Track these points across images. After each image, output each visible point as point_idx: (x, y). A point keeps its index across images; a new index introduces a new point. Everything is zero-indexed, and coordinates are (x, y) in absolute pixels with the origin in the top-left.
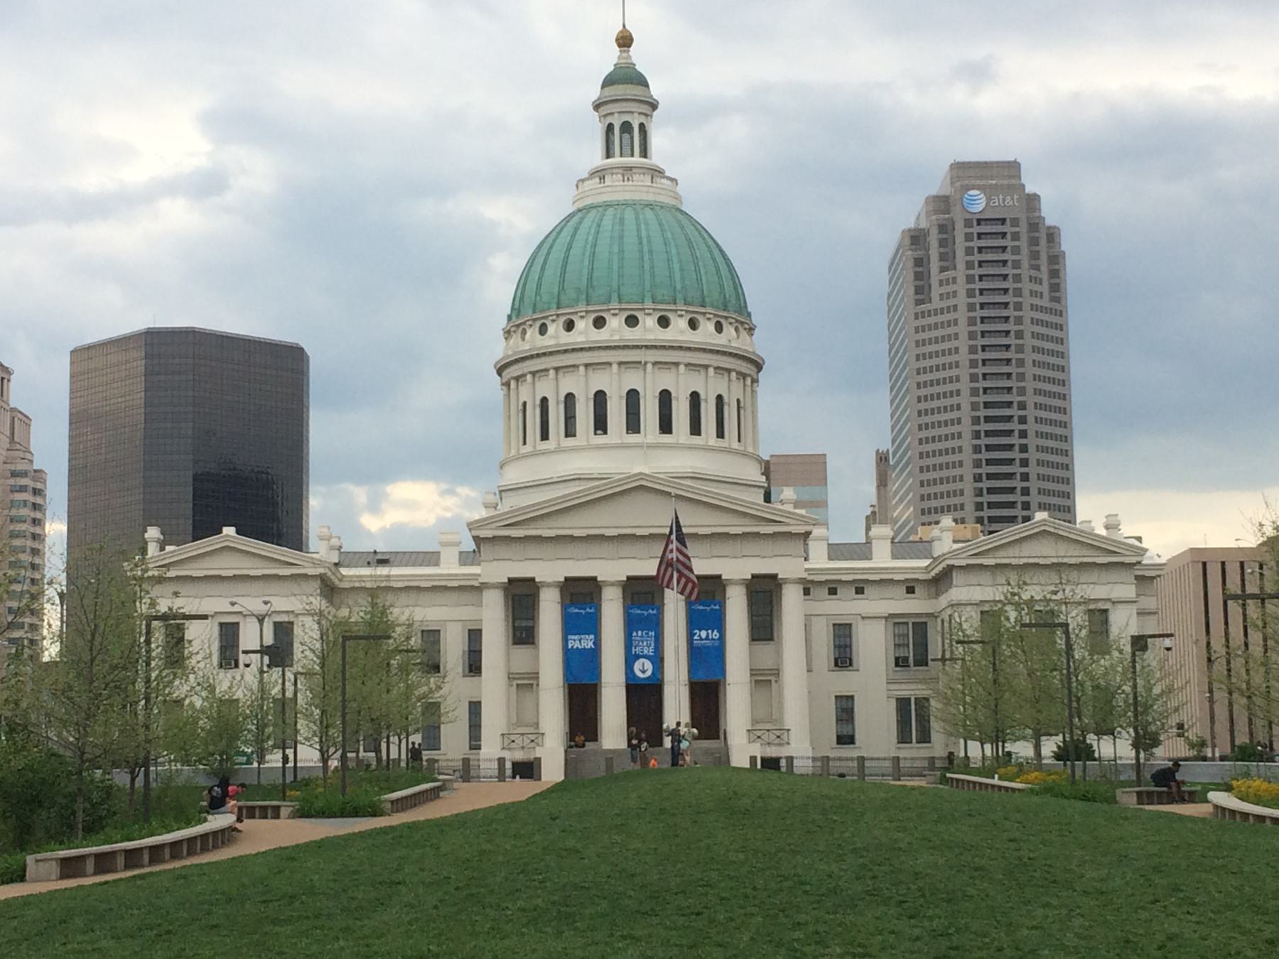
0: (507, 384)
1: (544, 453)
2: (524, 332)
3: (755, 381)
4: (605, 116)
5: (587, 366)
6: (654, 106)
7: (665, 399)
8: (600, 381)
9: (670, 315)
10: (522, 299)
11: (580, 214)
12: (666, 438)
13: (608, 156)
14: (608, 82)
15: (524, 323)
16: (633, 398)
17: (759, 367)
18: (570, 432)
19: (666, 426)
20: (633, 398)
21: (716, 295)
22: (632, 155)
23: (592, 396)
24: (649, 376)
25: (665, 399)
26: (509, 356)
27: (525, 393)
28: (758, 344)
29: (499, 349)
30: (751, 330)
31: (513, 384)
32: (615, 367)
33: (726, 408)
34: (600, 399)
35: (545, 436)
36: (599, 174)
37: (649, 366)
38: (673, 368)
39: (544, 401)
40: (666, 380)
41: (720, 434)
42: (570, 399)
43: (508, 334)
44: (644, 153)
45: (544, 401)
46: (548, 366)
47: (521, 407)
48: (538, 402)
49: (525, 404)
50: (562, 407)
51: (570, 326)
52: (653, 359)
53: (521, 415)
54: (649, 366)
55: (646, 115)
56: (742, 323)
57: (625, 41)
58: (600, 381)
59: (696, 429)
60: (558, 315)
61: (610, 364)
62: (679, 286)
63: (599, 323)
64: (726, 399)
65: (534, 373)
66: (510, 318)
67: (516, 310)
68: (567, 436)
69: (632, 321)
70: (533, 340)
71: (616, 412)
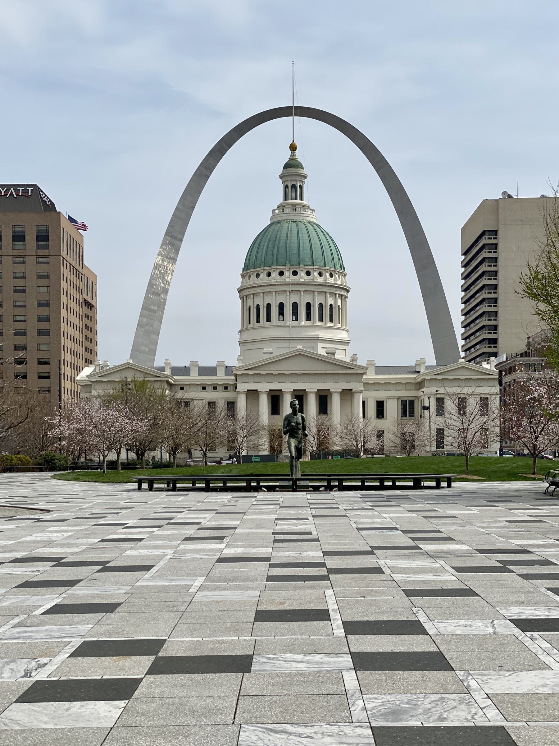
0: (242, 298)
1: (257, 328)
2: (250, 277)
3: (346, 297)
5: (276, 292)
6: (305, 177)
7: (308, 306)
8: (281, 299)
9: (311, 271)
10: (249, 262)
11: (273, 226)
12: (309, 323)
13: (285, 200)
14: (287, 166)
15: (250, 272)
16: (295, 306)
17: (348, 291)
18: (269, 319)
19: (309, 317)
20: (295, 306)
21: (330, 262)
22: (296, 199)
23: (278, 304)
24: (302, 297)
25: (308, 306)
26: (244, 286)
27: (250, 302)
28: (348, 282)
29: (238, 282)
30: (345, 275)
31: (245, 298)
33: (334, 309)
34: (281, 306)
35: (258, 321)
36: (281, 207)
37: (302, 293)
38: (312, 293)
39: (258, 306)
40: (308, 298)
41: (331, 321)
42: (269, 306)
43: (243, 276)
44: (301, 199)
45: (258, 306)
46: (259, 291)
48: (255, 306)
49: (250, 307)
50: (265, 309)
51: (269, 275)
53: (248, 311)
54: (302, 293)
56: (341, 273)
57: (293, 148)
59: (321, 319)
60: (264, 270)
61: (286, 291)
63: (281, 274)
64: (334, 306)
65: (253, 294)
66: (244, 269)
68: (267, 321)
69: (295, 273)
71: (288, 310)
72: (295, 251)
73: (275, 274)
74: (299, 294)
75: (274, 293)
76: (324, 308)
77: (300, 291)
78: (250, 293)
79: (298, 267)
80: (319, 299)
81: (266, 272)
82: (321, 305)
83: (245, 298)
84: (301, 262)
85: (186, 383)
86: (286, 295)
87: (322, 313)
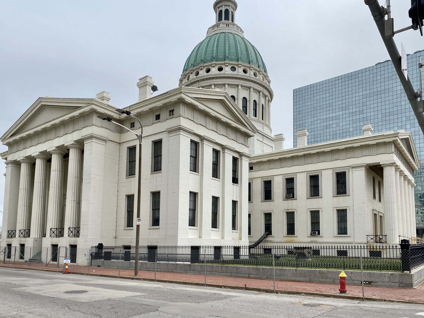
4: (219, 8)
9: (248, 69)
24: (240, 91)
32: (227, 86)
36: (217, 25)
37: (240, 87)
44: (233, 20)
51: (208, 71)
52: (241, 84)
55: (234, 9)
60: (204, 67)
61: (224, 85)
62: (250, 60)
63: (220, 69)
67: (185, 70)
69: (233, 69)
70: (193, 77)
72: (233, 50)
73: (214, 71)
75: (213, 86)
77: (237, 86)
79: (236, 63)
81: (205, 69)
84: (239, 59)
86: (225, 88)
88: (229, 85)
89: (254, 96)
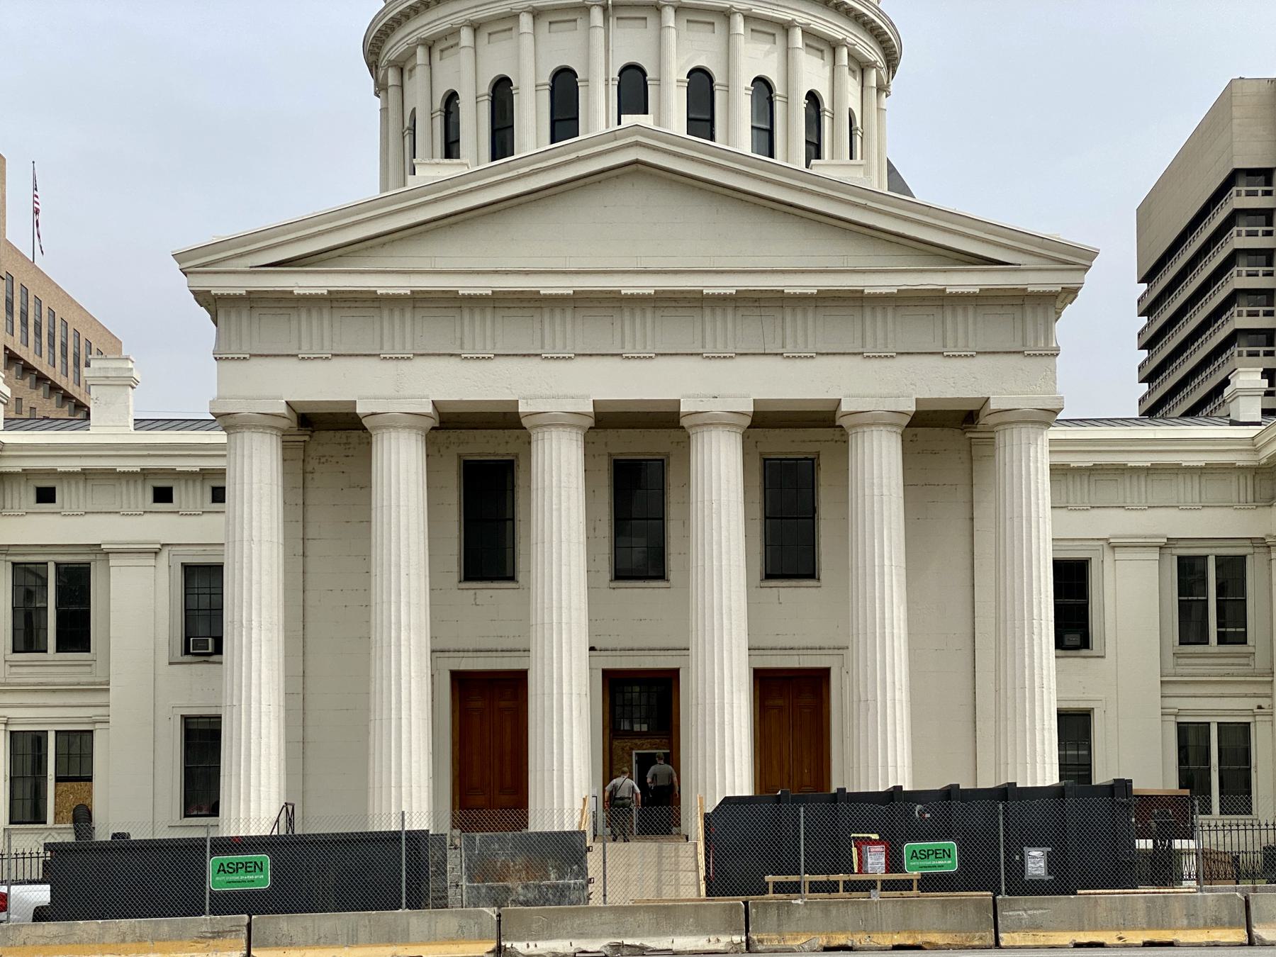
0: (381, 88)
23: (546, 79)
24: (672, 34)
34: (564, 88)
38: (719, 27)
42: (502, 92)
45: (452, 97)
47: (407, 124)
50: (485, 108)
58: (560, 48)
74: (652, 21)
75: (526, 21)
76: (779, 107)
78: (413, 38)
80: (755, 58)
82: (762, 85)
83: (392, 77)
85: (63, 465)
86: (589, 27)
87: (771, 132)
88: (605, 9)
89: (755, 58)
